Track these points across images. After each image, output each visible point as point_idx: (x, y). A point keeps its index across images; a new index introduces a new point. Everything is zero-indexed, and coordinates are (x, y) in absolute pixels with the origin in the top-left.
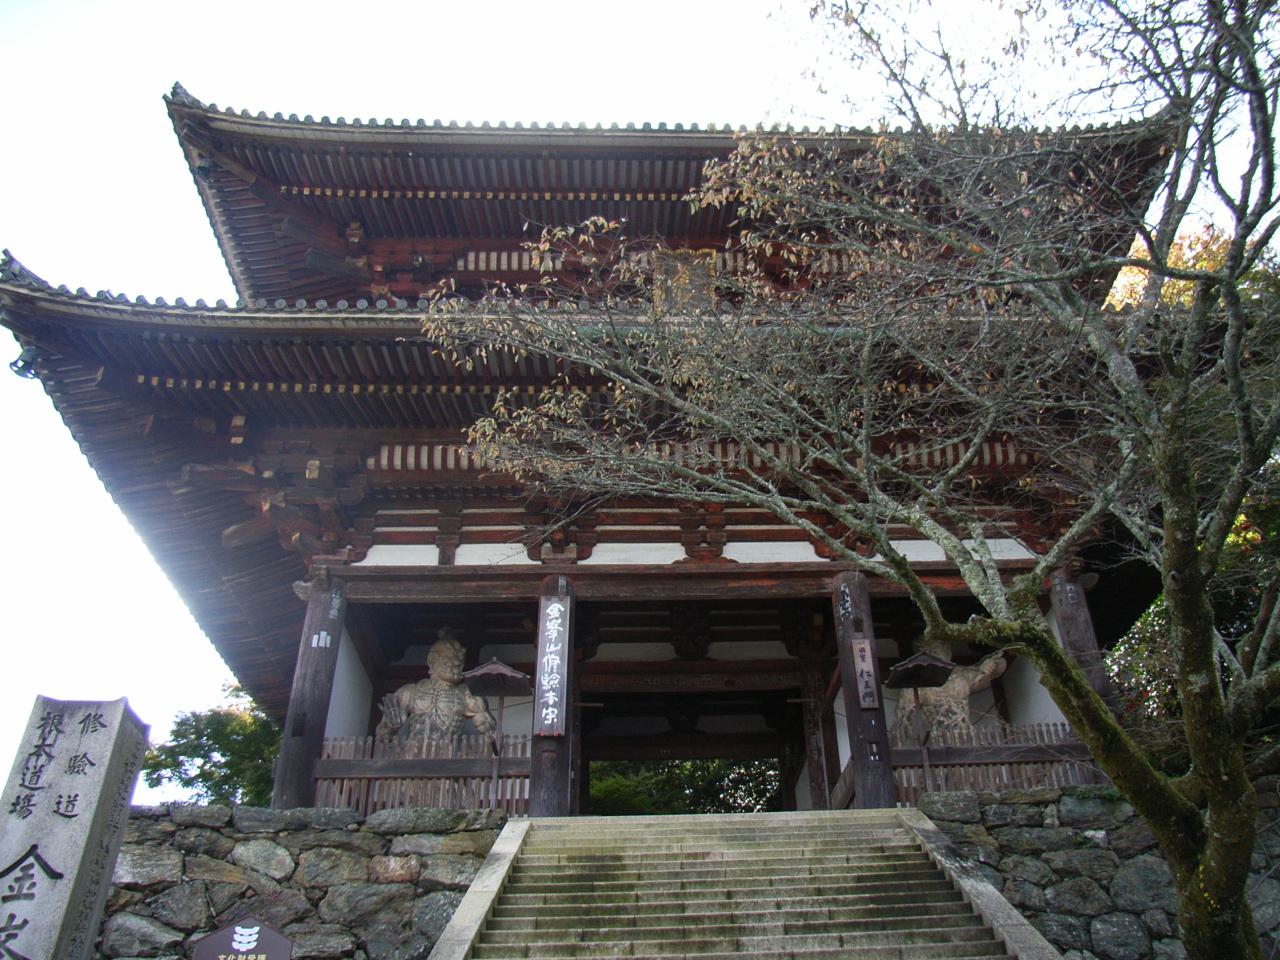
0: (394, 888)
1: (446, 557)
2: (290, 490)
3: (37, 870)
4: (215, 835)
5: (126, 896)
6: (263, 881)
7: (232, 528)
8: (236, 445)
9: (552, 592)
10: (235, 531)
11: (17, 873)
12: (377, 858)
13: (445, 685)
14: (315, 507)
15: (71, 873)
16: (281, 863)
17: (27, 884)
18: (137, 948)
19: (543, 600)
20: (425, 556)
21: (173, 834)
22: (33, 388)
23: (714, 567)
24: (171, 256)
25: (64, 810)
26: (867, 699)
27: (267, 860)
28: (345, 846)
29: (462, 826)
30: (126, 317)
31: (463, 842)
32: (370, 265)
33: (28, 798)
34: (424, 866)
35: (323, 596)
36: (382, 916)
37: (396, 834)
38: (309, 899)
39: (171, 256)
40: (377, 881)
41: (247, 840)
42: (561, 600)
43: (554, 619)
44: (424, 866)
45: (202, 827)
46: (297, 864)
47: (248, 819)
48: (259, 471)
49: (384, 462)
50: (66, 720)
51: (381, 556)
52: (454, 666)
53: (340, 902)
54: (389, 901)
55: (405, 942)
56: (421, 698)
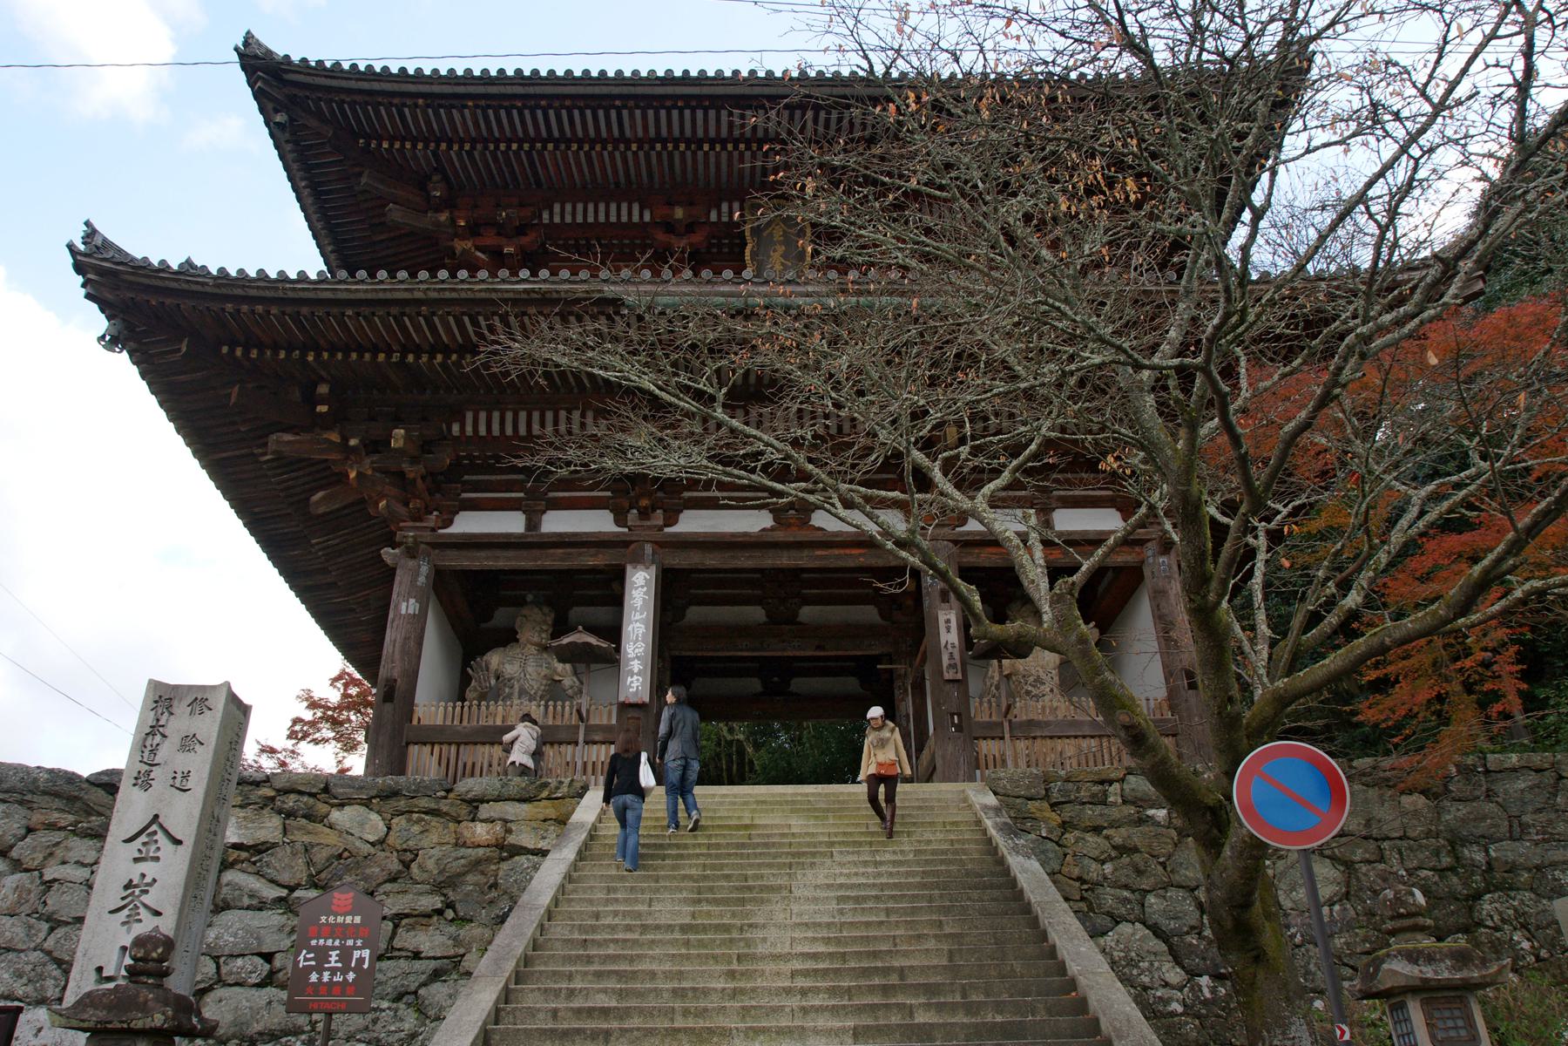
0: (481, 851)
1: (532, 525)
2: (375, 457)
3: (160, 836)
4: (311, 800)
5: (234, 854)
6: (358, 843)
7: (320, 494)
8: (321, 414)
9: (638, 560)
10: (323, 498)
11: (143, 838)
12: (464, 824)
13: (533, 650)
14: (401, 475)
15: (189, 842)
16: (375, 827)
17: (153, 847)
18: (246, 901)
19: (629, 568)
20: (511, 523)
21: (273, 799)
22: (122, 364)
23: (802, 535)
24: (252, 224)
26: (952, 671)
27: (361, 825)
29: (545, 794)
30: (208, 289)
31: (546, 809)
32: (453, 221)
33: (148, 773)
34: (509, 831)
35: (411, 563)
36: (470, 878)
37: (482, 801)
38: (402, 862)
39: (252, 224)
40: (464, 845)
41: (341, 806)
43: (640, 587)
44: (509, 831)
45: (301, 793)
46: (389, 829)
47: (342, 786)
48: (345, 439)
49: (469, 430)
50: (175, 703)
51: (468, 524)
52: (542, 631)
53: (430, 864)
54: (476, 864)
55: (491, 902)
56: (510, 662)
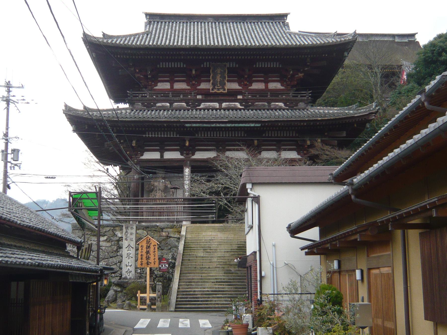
24: (98, 98)
27: (143, 233)
28: (155, 231)
39: (98, 98)
42: (188, 168)
43: (187, 171)
51: (148, 156)
54: (164, 240)
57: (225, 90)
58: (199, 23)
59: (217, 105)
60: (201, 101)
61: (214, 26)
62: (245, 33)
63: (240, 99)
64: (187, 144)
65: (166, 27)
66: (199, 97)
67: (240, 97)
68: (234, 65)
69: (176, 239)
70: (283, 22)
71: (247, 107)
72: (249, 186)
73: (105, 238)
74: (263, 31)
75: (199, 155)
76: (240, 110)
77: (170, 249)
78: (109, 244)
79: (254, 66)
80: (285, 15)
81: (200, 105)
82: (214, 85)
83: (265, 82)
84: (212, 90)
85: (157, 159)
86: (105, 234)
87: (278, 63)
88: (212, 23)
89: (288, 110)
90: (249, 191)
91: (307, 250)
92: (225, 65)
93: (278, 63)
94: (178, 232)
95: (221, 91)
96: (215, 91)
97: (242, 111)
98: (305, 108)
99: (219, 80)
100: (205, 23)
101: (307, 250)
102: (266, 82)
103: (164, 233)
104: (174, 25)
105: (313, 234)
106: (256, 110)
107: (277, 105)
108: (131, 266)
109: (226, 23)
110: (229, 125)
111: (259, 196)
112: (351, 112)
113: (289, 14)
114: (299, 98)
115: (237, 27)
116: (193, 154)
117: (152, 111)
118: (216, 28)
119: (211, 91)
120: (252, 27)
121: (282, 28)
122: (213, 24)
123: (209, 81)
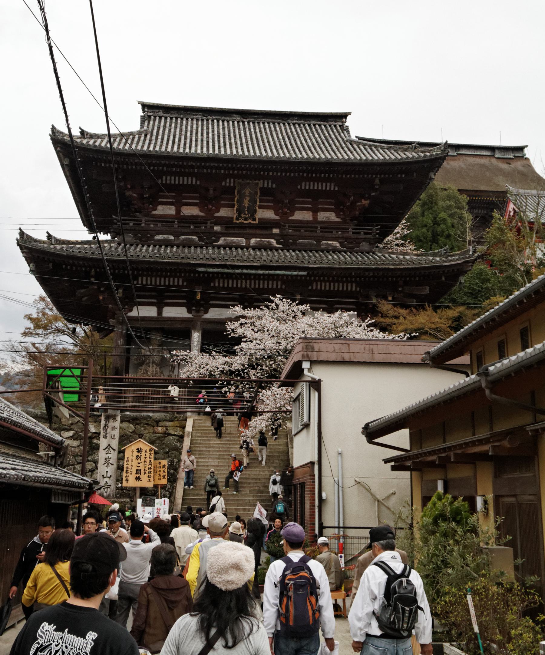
5: (95, 435)
9: (195, 329)
15: (117, 450)
25: (113, 437)
28: (147, 424)
31: (176, 423)
42: (198, 332)
43: (196, 336)
54: (159, 438)
57: (254, 220)
58: (221, 122)
59: (243, 241)
60: (218, 235)
61: (241, 127)
62: (287, 139)
63: (276, 234)
64: (198, 297)
65: (173, 125)
66: (217, 228)
67: (276, 231)
68: (270, 184)
69: (177, 438)
70: (340, 126)
71: (286, 247)
72: (306, 365)
73: (71, 433)
74: (312, 137)
75: (213, 314)
76: (277, 249)
77: (167, 453)
78: (75, 443)
79: (299, 187)
80: (345, 116)
81: (218, 241)
82: (240, 211)
83: (313, 212)
84: (237, 219)
85: (153, 317)
86: (72, 427)
87: (332, 184)
88: (238, 122)
89: (345, 252)
90: (306, 372)
91: (393, 464)
92: (257, 184)
93: (332, 184)
94: (180, 427)
95: (250, 221)
96: (241, 220)
97: (280, 251)
98: (371, 251)
99: (247, 205)
100: (228, 122)
101: (393, 464)
102: (315, 211)
103: (160, 429)
104: (184, 122)
105: (401, 438)
106: (299, 251)
107: (330, 245)
108: (109, 477)
109: (259, 123)
110: (261, 272)
111: (320, 380)
112: (438, 259)
113: (349, 113)
114: (362, 236)
115: (276, 130)
116: (206, 312)
117: (149, 246)
118: (244, 129)
119: (235, 221)
120: (296, 131)
121: (339, 134)
122: (241, 124)
123: (233, 206)
